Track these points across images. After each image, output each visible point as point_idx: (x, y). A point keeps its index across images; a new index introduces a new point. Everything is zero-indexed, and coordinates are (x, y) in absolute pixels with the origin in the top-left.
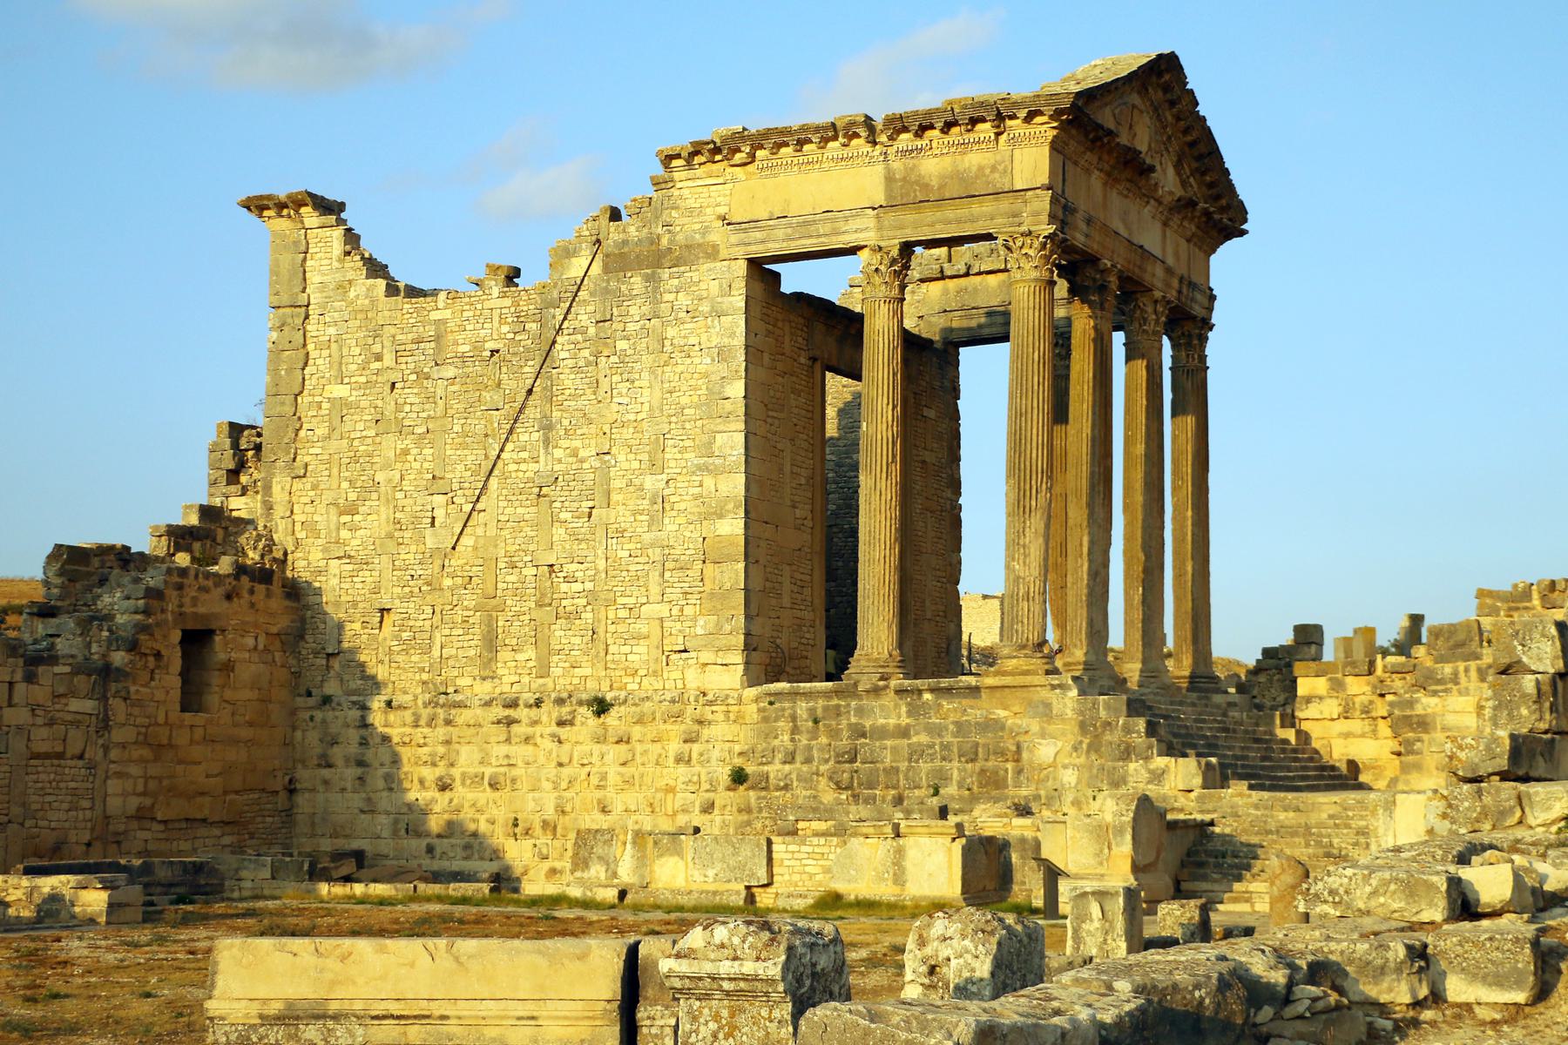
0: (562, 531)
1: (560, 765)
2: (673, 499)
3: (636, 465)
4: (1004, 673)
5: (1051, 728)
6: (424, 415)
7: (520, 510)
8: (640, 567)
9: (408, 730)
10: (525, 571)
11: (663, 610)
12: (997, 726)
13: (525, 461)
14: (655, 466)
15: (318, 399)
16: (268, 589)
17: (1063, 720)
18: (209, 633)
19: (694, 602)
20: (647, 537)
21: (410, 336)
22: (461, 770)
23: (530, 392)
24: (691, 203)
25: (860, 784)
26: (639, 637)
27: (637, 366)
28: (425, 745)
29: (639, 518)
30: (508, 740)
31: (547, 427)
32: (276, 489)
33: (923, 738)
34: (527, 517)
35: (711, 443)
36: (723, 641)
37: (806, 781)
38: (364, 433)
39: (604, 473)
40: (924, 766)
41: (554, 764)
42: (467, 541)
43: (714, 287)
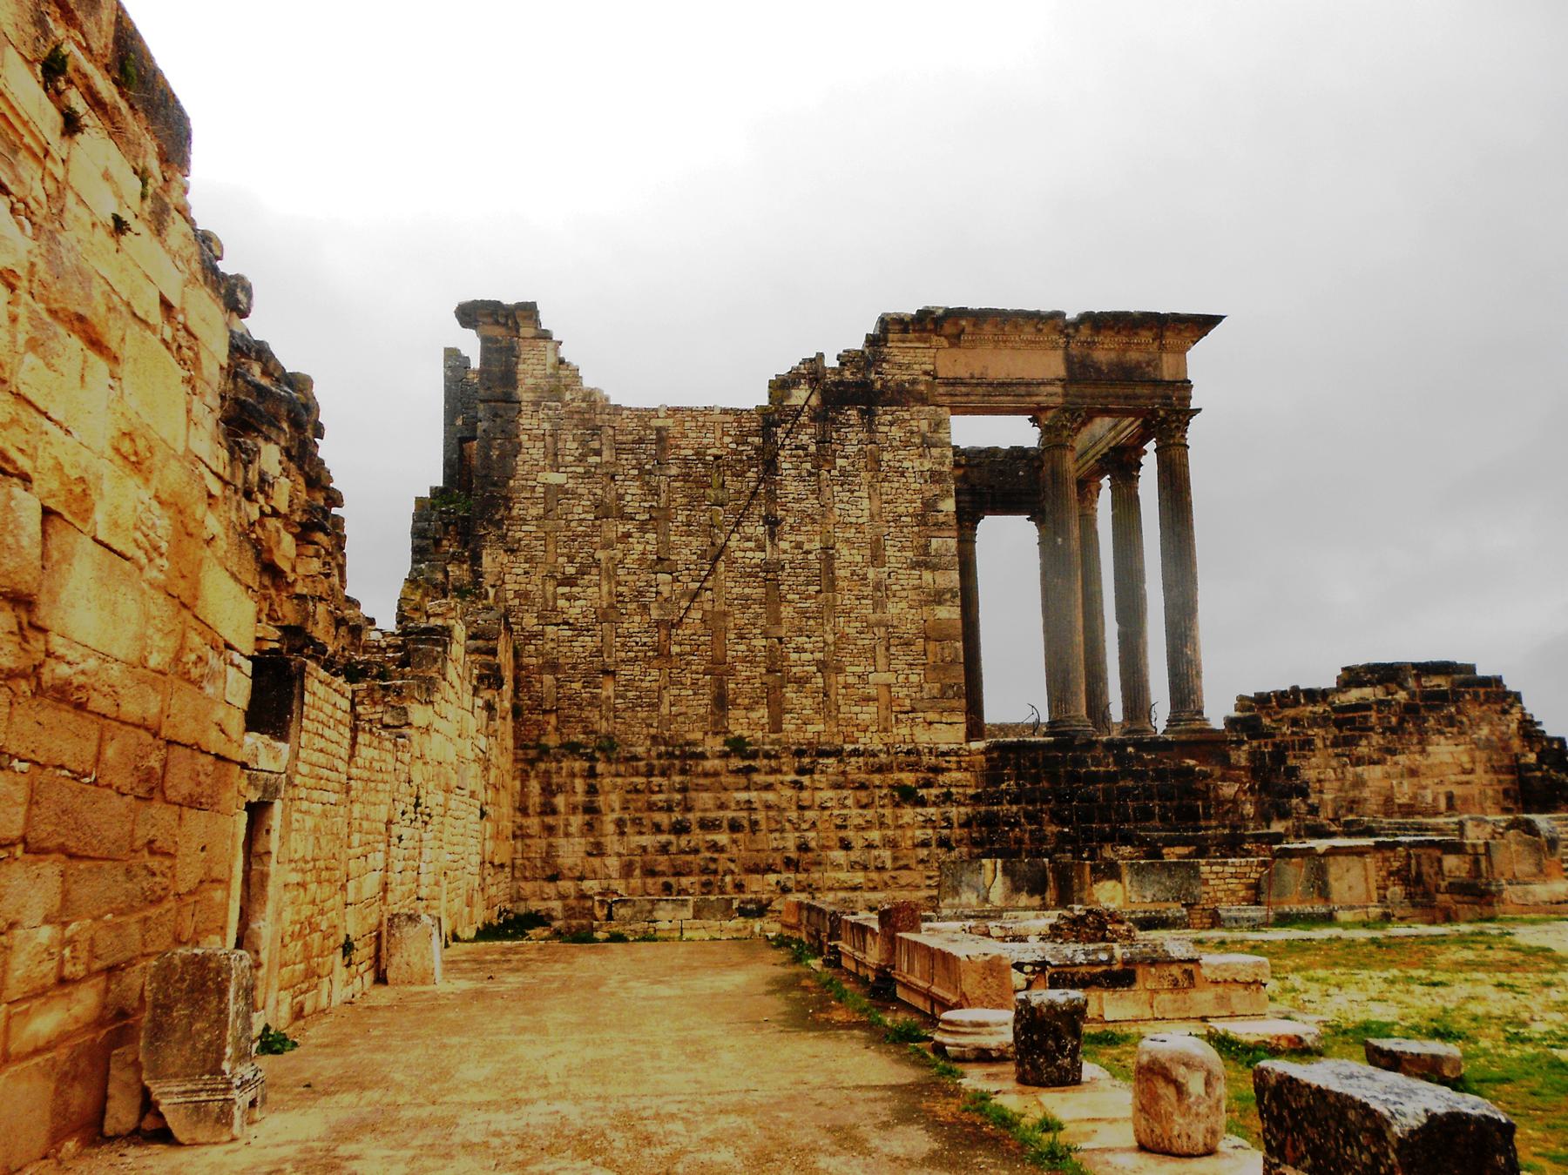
0: (790, 609)
3: (859, 559)
6: (647, 505)
7: (747, 591)
8: (867, 642)
9: (643, 780)
10: (754, 642)
11: (889, 678)
13: (751, 550)
15: (534, 483)
20: (873, 618)
21: (630, 437)
22: (699, 814)
24: (899, 359)
26: (868, 699)
30: (747, 788)
31: (772, 523)
32: (486, 561)
34: (754, 596)
35: (927, 546)
37: (1031, 817)
38: (582, 516)
41: (794, 807)
43: (924, 426)
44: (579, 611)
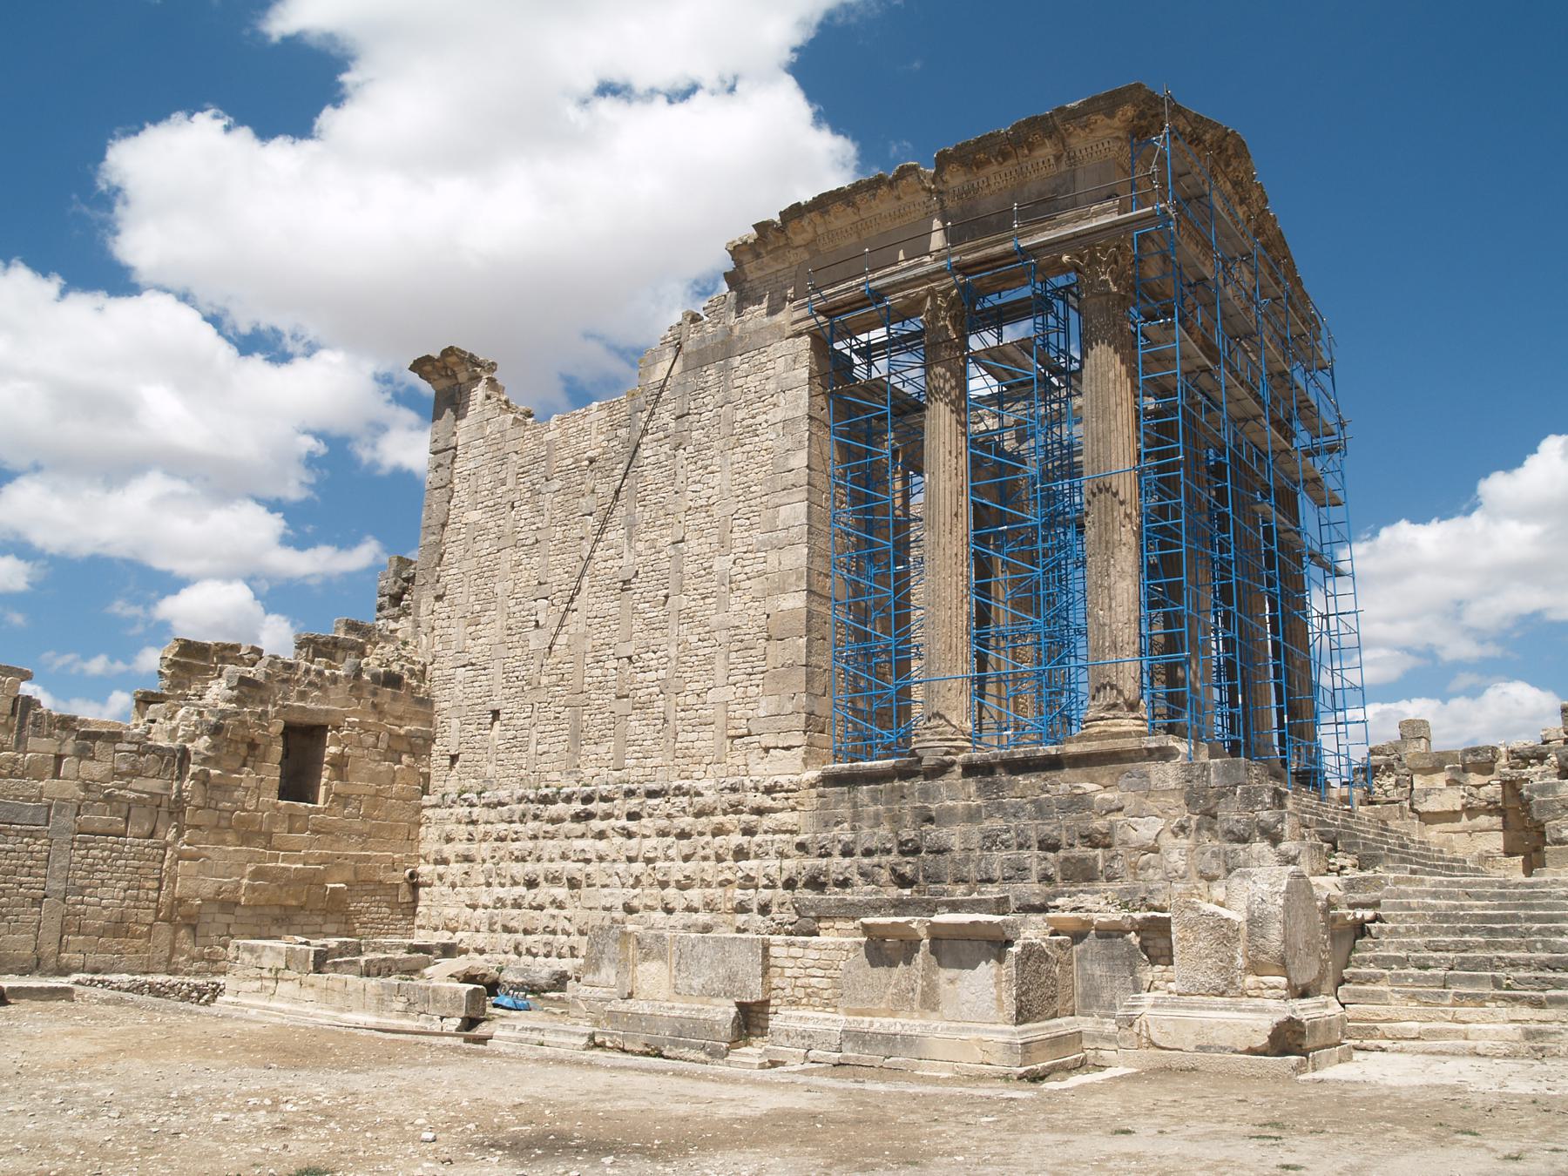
1: (630, 860)
2: (739, 577)
3: (706, 548)
4: (1089, 738)
5: (1149, 803)
8: (707, 651)
11: (728, 693)
12: (1079, 803)
14: (724, 545)
16: (394, 693)
17: (1165, 792)
18: (323, 729)
19: (757, 682)
20: (715, 620)
23: (617, 492)
25: (926, 878)
27: (710, 453)
28: (517, 840)
29: (707, 601)
32: (423, 608)
33: (997, 823)
36: (784, 723)
39: (678, 559)
40: (999, 856)
41: (624, 858)
42: (562, 639)
44: (478, 649)
